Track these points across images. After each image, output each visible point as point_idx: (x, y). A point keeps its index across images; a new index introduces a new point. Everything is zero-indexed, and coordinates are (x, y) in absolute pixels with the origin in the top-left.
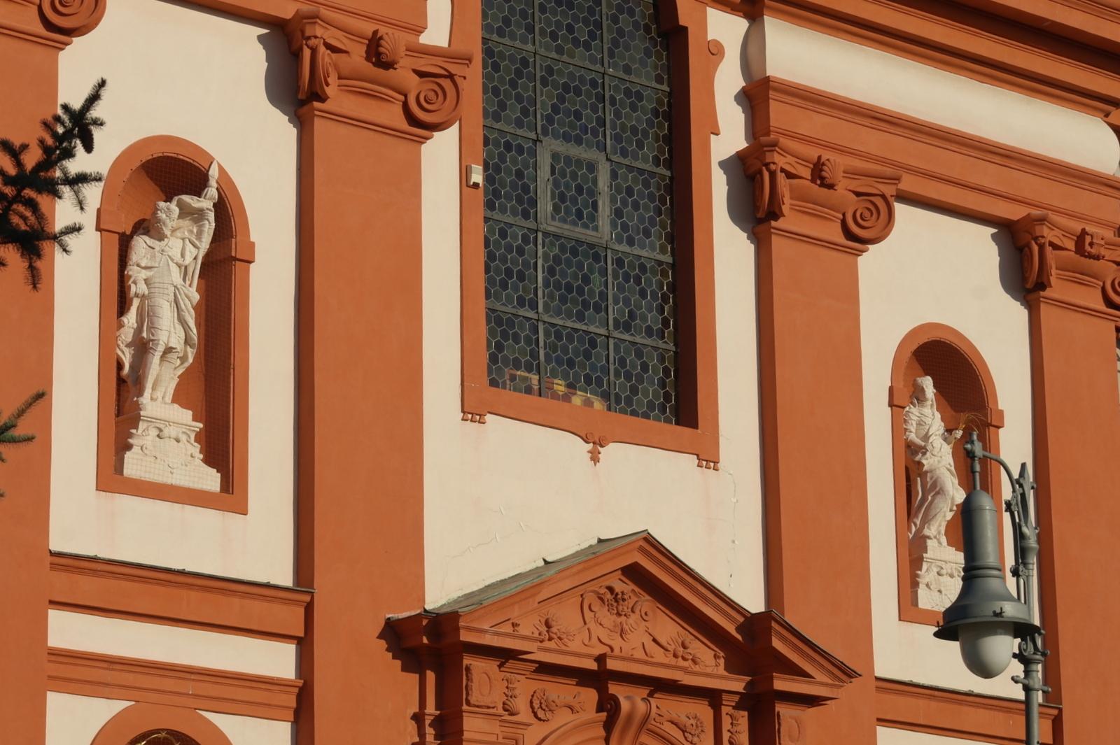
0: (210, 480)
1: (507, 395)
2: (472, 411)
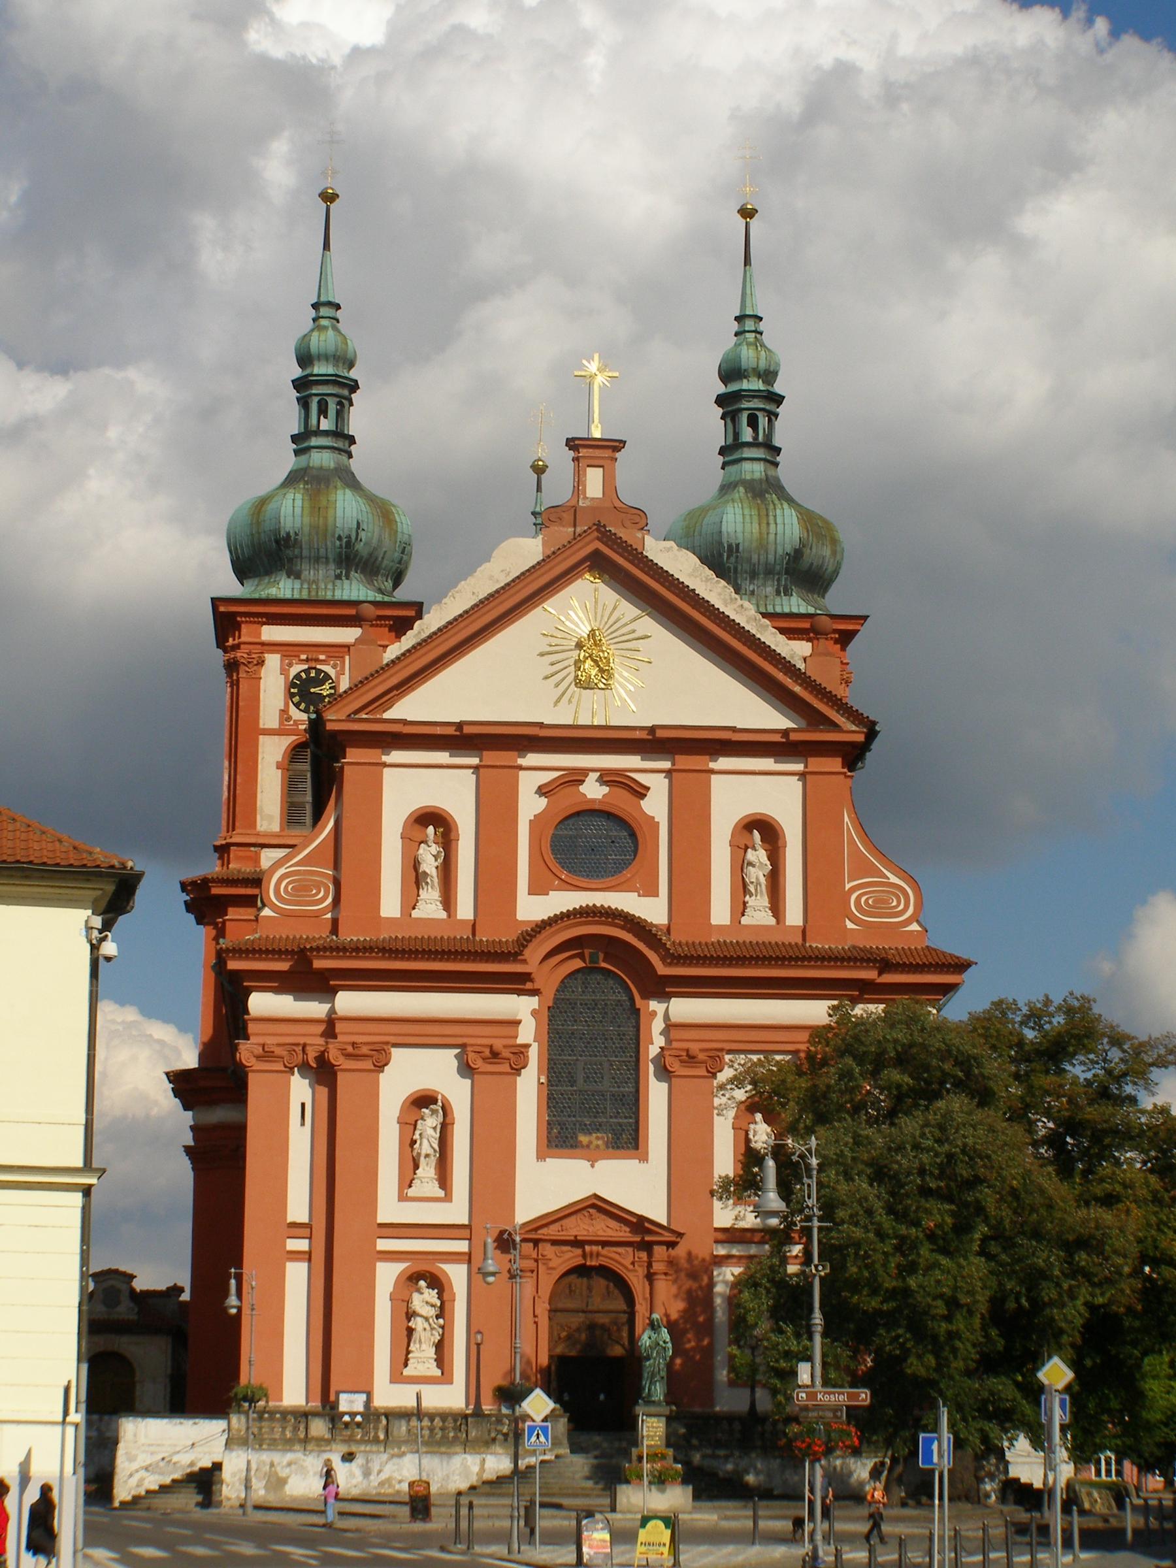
0: (441, 1194)
2: (541, 1156)
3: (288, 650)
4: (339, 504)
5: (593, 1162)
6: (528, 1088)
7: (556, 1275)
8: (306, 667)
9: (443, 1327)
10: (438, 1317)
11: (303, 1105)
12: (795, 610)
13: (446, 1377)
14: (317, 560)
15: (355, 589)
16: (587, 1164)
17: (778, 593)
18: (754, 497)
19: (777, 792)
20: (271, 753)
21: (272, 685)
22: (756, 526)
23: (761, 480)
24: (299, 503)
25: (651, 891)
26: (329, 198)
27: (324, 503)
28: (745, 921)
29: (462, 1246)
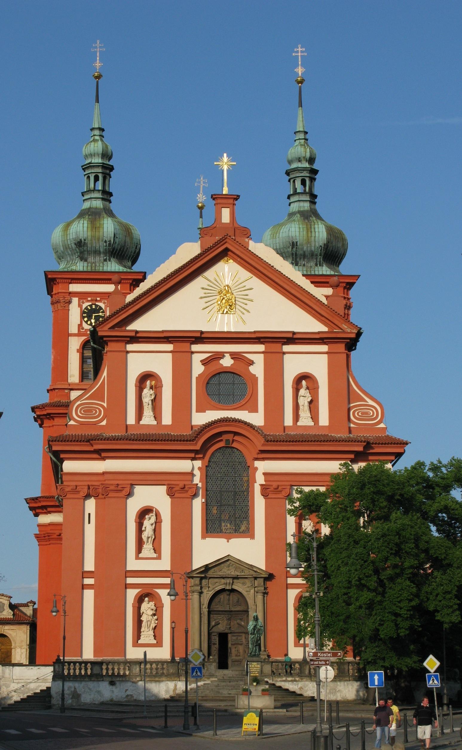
0: (155, 555)
1: (209, 534)
2: (203, 537)
3: (83, 296)
4: (105, 226)
5: (228, 539)
6: (198, 504)
7: (211, 593)
8: (90, 303)
9: (157, 620)
10: (154, 615)
11: (89, 514)
12: (325, 273)
13: (159, 644)
14: (97, 252)
15: (113, 266)
16: (225, 540)
17: (316, 265)
18: (304, 219)
19: (314, 362)
20: (75, 344)
22: (305, 233)
23: (308, 211)
24: (86, 225)
25: (254, 410)
26: (99, 77)
27: (98, 225)
28: (299, 424)
29: (167, 581)
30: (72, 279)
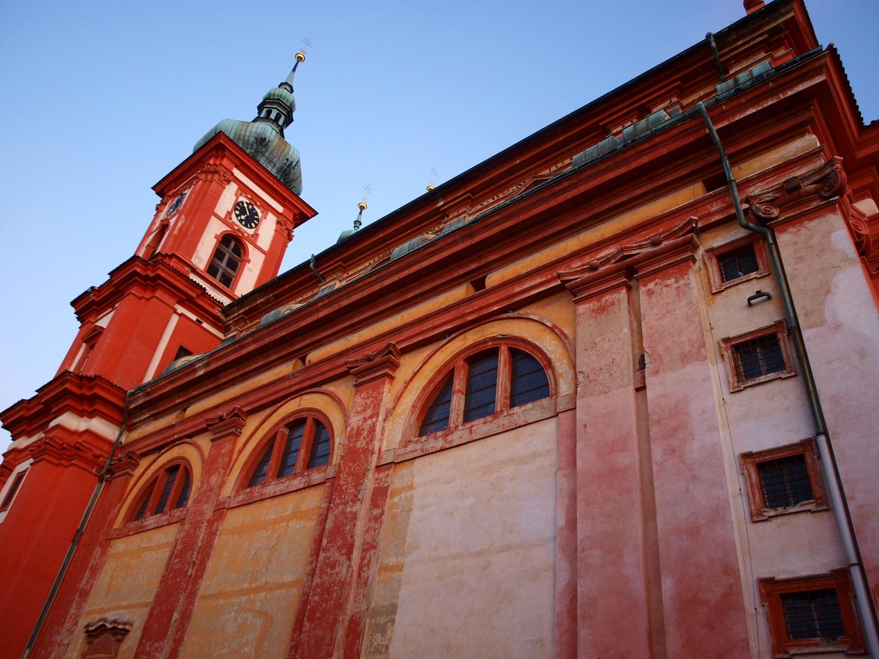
20: (214, 229)
21: (228, 198)
26: (300, 59)
30: (243, 163)
